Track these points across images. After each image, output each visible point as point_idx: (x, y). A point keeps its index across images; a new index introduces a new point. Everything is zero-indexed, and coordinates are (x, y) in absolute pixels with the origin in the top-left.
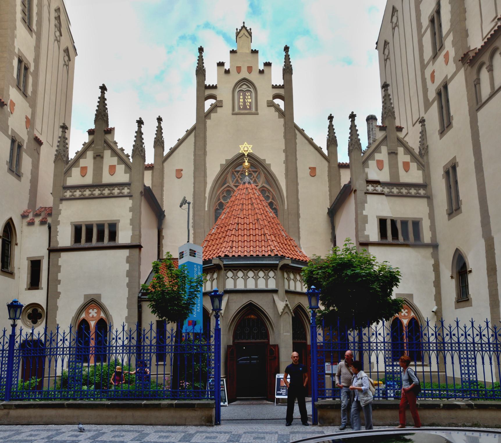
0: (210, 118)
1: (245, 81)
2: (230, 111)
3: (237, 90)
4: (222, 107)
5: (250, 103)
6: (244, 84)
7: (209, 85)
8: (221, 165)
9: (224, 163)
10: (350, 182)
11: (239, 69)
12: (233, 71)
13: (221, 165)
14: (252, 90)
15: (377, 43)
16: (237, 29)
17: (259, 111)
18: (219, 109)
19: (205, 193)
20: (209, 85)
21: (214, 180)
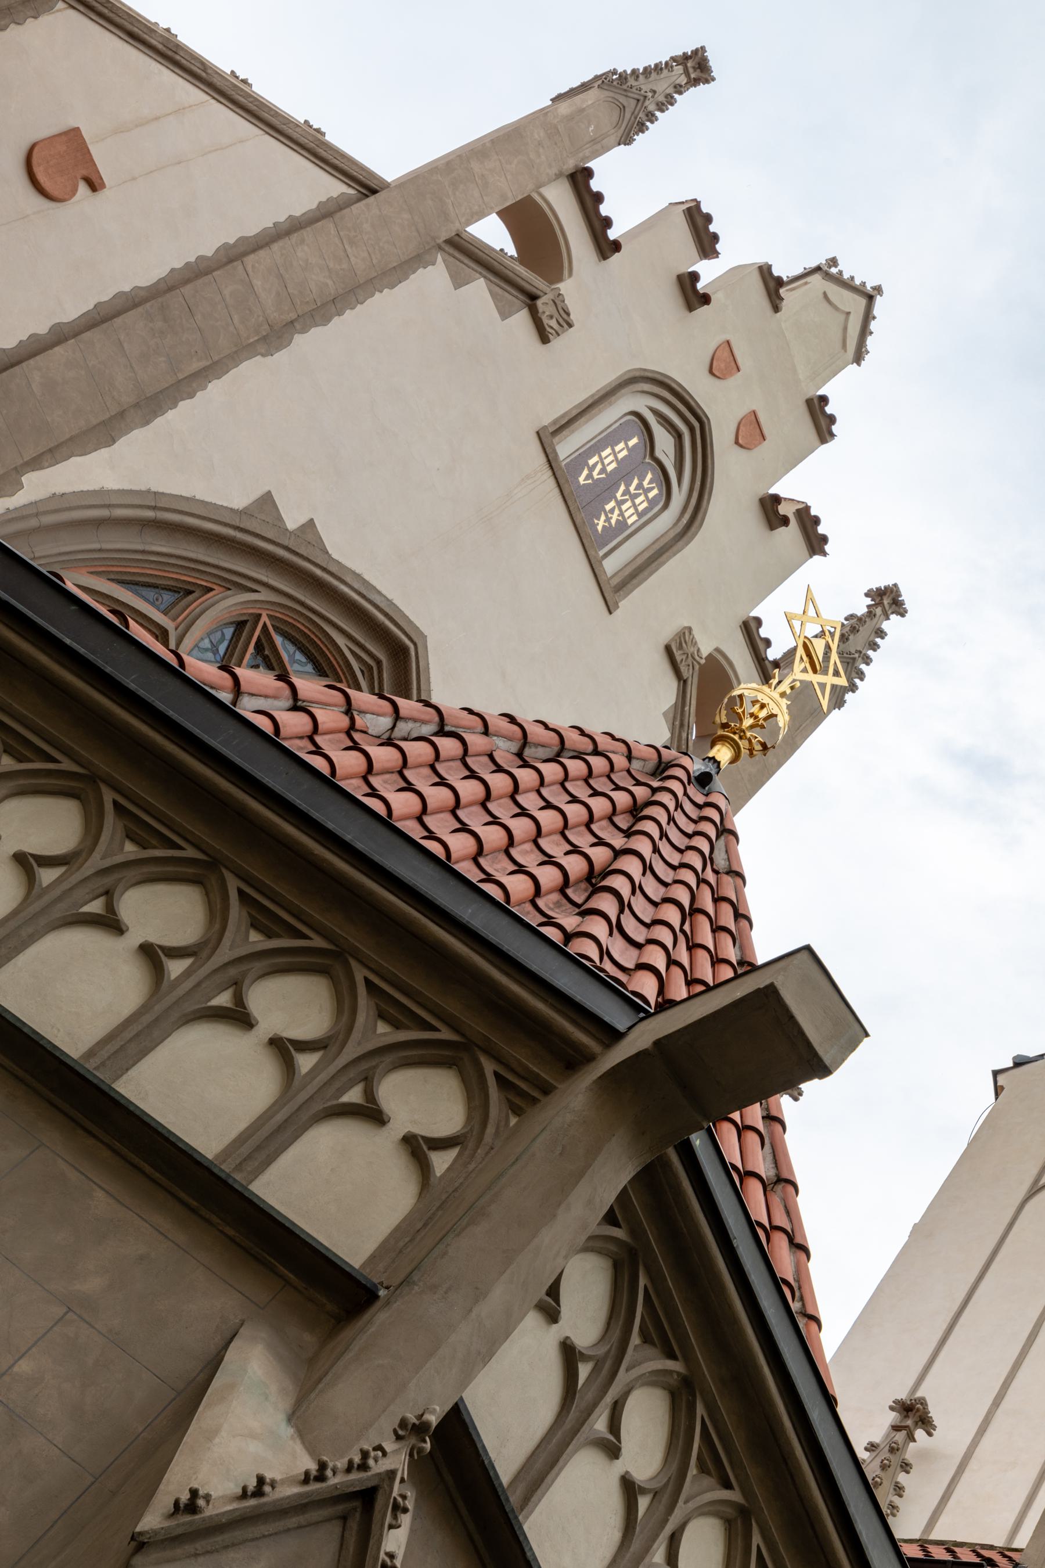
0: (458, 282)
1: (694, 426)
2: (548, 416)
3: (642, 404)
4: (544, 337)
5: (622, 524)
6: (679, 436)
7: (598, 198)
8: (267, 500)
9: (292, 521)
10: (721, 1518)
11: (722, 363)
12: (707, 328)
13: (267, 500)
14: (678, 497)
15: (1020, 1062)
16: (833, 262)
17: (626, 605)
18: (522, 317)
19: (36, 463)
20: (598, 198)
21: (154, 499)
